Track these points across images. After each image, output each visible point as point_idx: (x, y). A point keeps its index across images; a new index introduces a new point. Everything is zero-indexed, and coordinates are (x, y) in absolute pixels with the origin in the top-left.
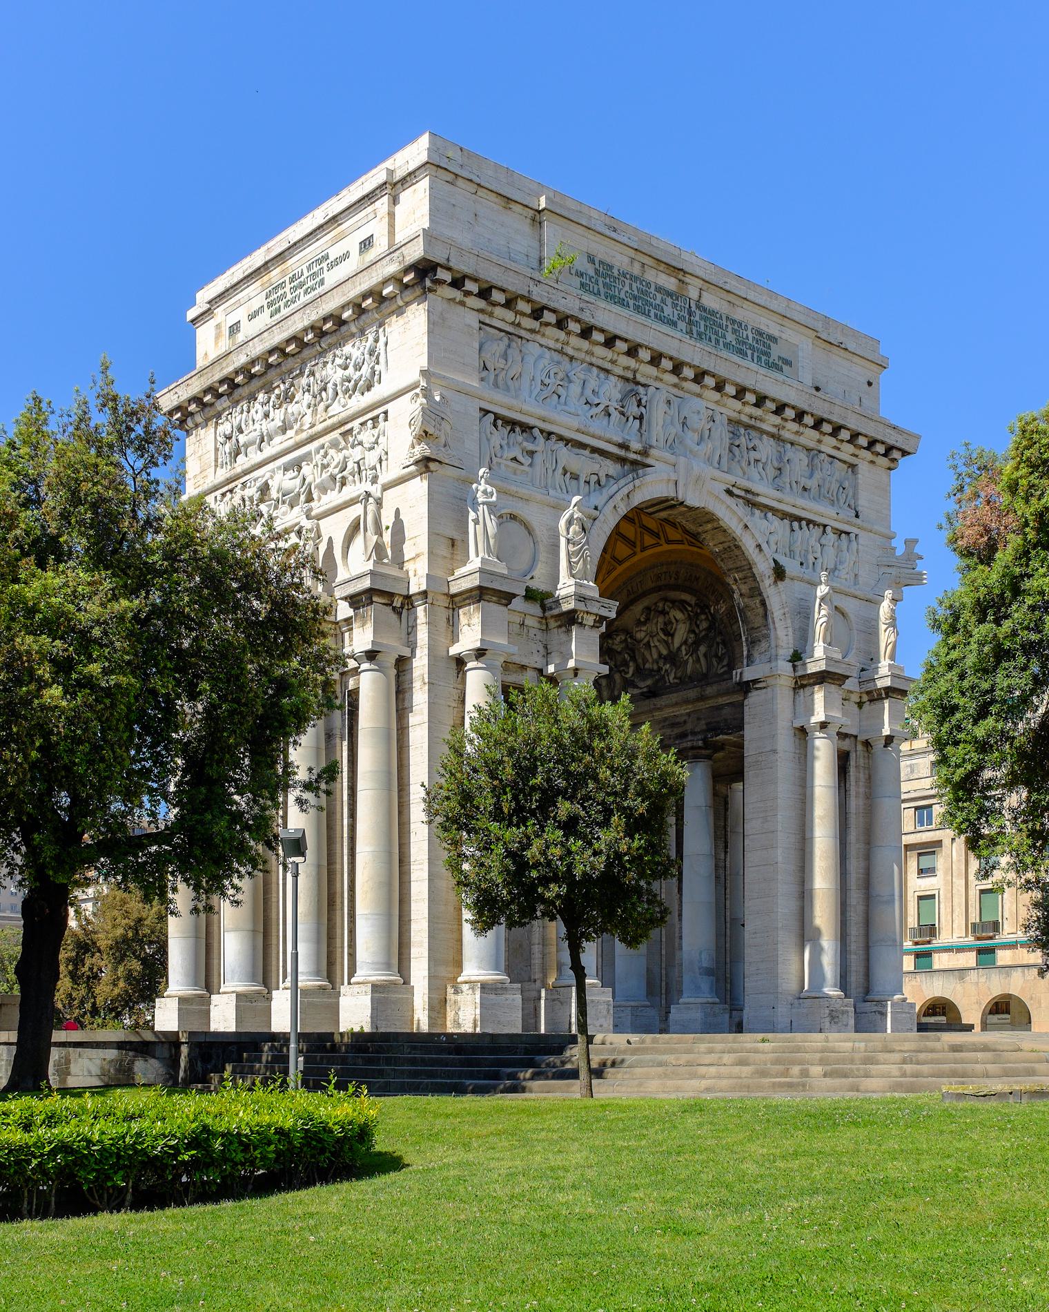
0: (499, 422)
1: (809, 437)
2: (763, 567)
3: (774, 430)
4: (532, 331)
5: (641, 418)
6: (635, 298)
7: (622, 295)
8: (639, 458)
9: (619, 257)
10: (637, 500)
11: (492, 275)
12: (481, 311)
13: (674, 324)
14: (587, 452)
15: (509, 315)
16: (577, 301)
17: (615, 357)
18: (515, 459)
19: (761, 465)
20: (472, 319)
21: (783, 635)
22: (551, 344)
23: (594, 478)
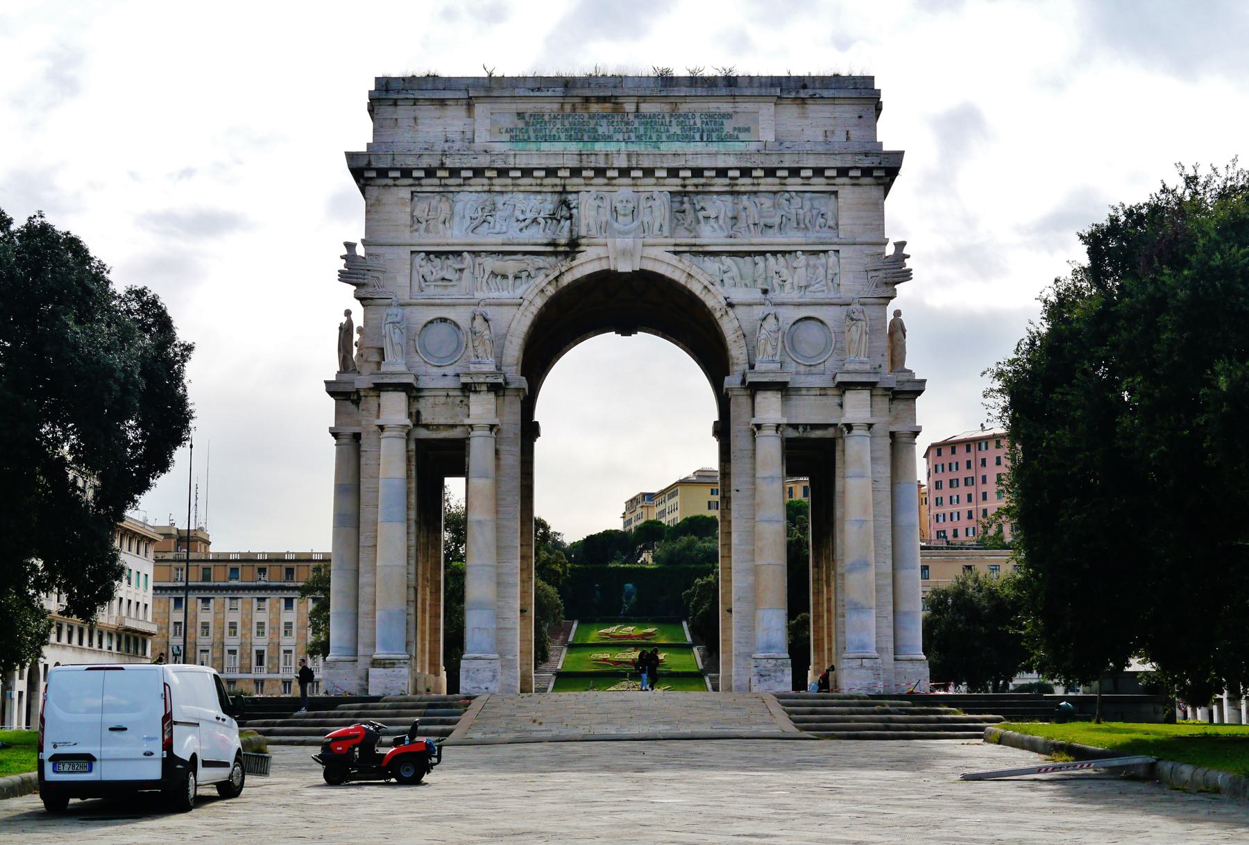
0: (432, 256)
1: (769, 184)
2: (713, 302)
3: (727, 189)
4: (460, 185)
5: (571, 217)
6: (567, 130)
7: (554, 132)
8: (567, 249)
9: (548, 106)
10: (567, 280)
11: (410, 162)
12: (410, 185)
13: (608, 139)
14: (519, 257)
15: (436, 181)
16: (488, 158)
17: (539, 181)
18: (443, 279)
19: (712, 221)
20: (405, 193)
21: (737, 352)
22: (479, 189)
23: (524, 274)
